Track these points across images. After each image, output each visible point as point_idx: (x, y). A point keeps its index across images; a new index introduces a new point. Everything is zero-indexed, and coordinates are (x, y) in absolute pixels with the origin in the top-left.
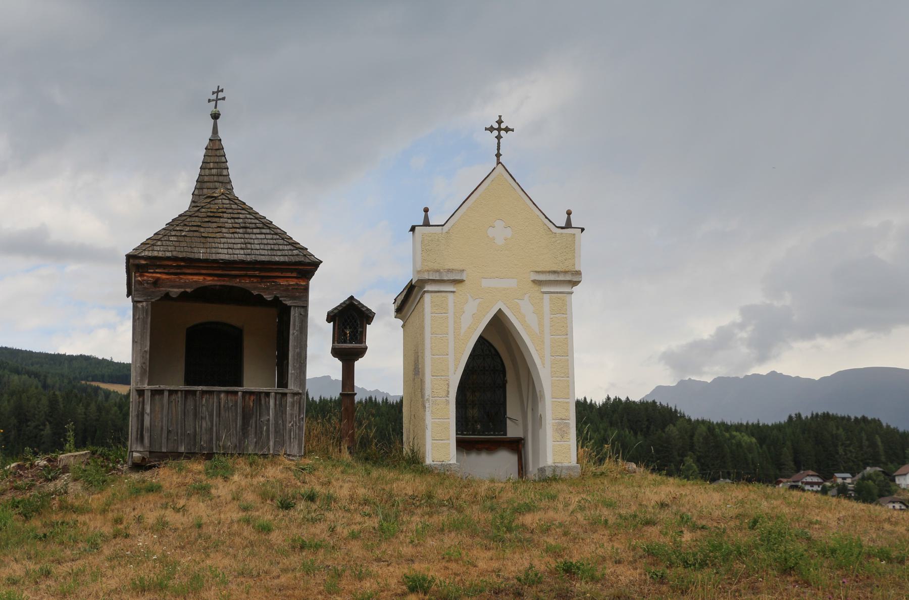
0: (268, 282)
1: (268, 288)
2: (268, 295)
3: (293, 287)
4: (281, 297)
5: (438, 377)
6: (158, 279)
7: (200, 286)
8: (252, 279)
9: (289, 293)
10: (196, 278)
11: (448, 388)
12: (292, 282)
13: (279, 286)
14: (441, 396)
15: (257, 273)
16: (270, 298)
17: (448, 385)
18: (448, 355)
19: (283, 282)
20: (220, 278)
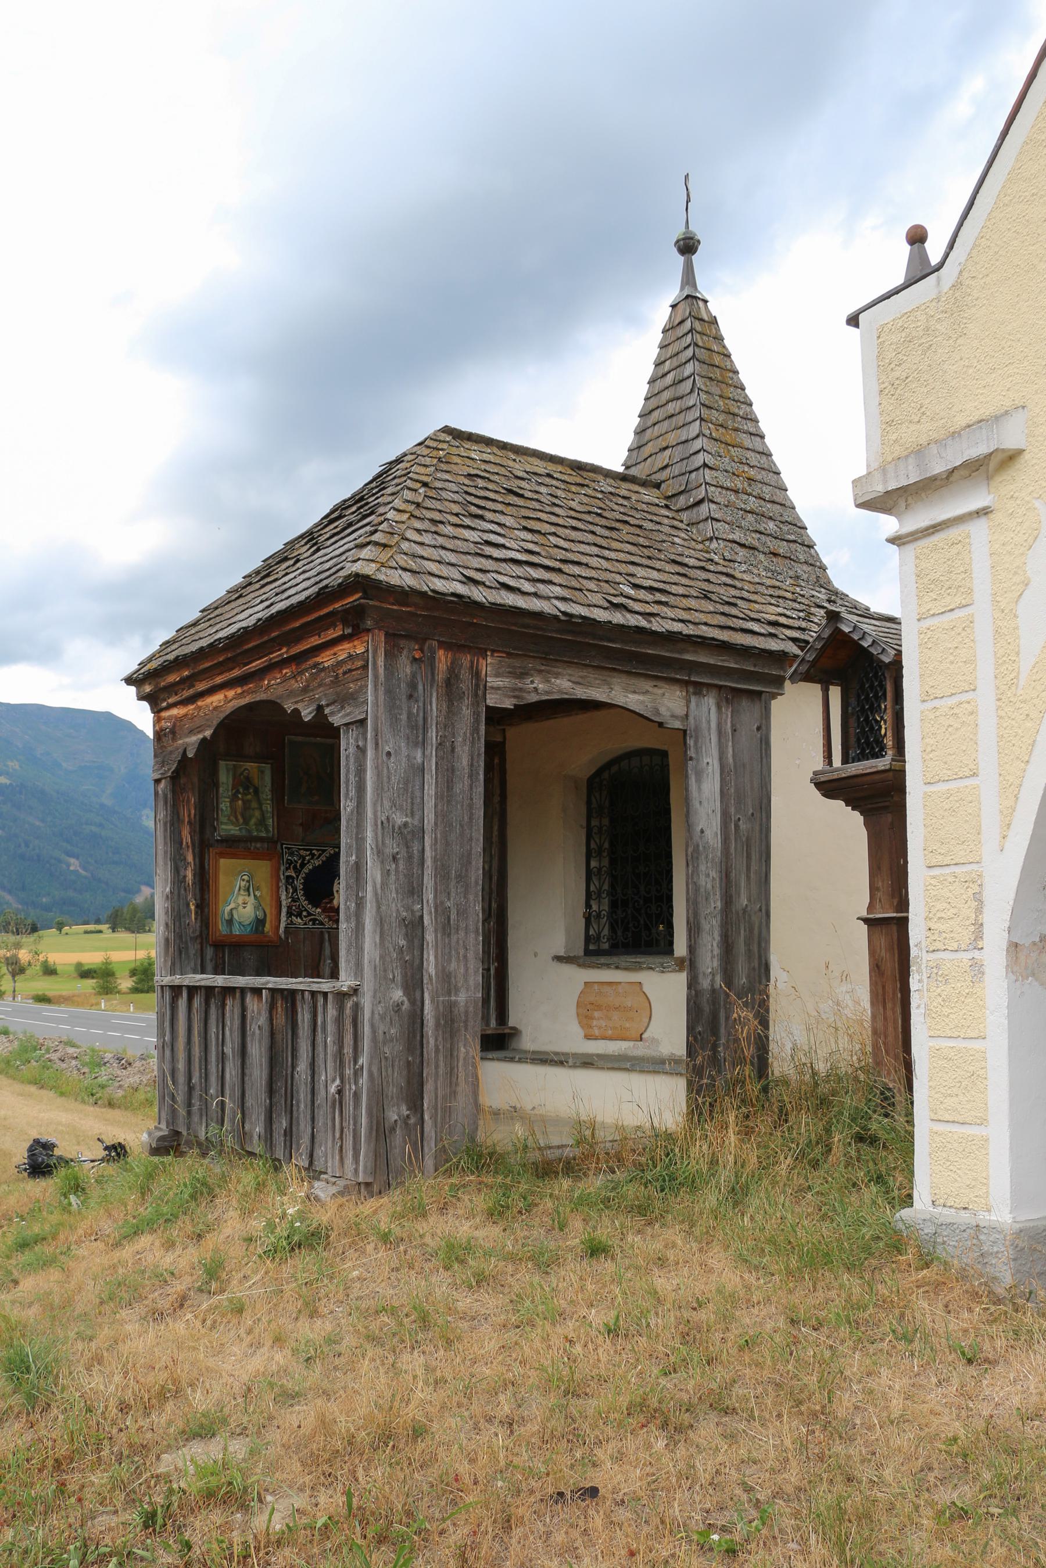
0: (306, 670)
1: (305, 690)
2: (308, 706)
3: (344, 668)
4: (328, 705)
5: (947, 871)
6: (180, 719)
7: (222, 716)
8: (284, 671)
9: (339, 689)
10: (216, 699)
11: (979, 910)
12: (343, 651)
13: (323, 674)
14: (955, 946)
15: (284, 652)
16: (310, 713)
17: (978, 898)
18: (975, 775)
19: (326, 659)
20: (245, 688)
